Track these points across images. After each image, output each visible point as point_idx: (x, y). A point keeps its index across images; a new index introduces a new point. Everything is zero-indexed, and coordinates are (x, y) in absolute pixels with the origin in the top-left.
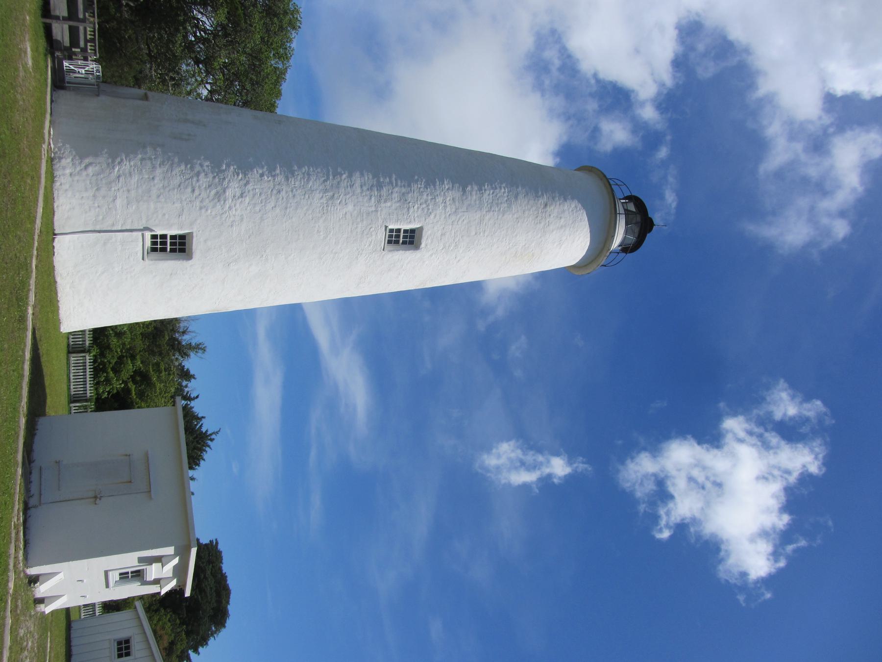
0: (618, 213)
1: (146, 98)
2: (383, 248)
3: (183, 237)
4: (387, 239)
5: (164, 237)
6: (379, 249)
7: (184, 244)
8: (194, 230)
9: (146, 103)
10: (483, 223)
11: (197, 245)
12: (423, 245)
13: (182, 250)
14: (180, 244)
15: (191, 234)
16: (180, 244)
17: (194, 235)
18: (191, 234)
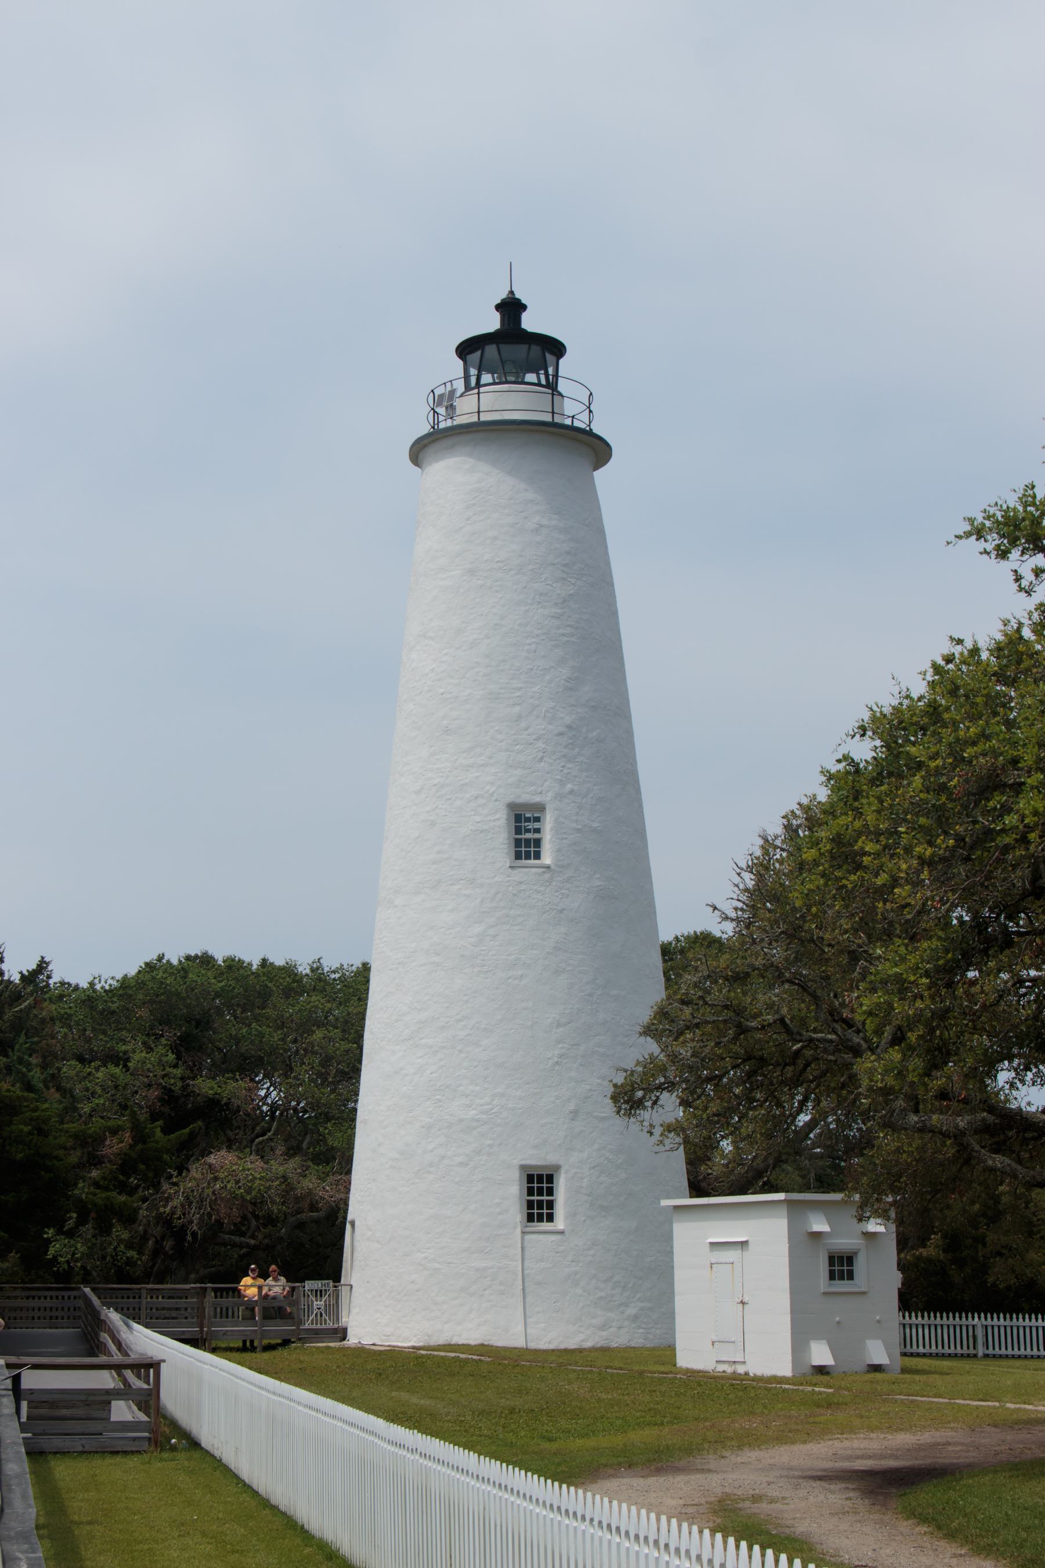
0: (475, 419)
1: (353, 1224)
2: (543, 870)
3: (530, 1178)
4: (532, 862)
5: (530, 1205)
6: (547, 876)
7: (540, 1178)
8: (517, 1161)
9: (357, 1224)
10: (500, 693)
11: (539, 1158)
12: (537, 799)
13: (550, 1178)
14: (540, 1181)
15: (523, 1168)
16: (540, 1181)
17: (524, 1163)
18: (523, 1168)
